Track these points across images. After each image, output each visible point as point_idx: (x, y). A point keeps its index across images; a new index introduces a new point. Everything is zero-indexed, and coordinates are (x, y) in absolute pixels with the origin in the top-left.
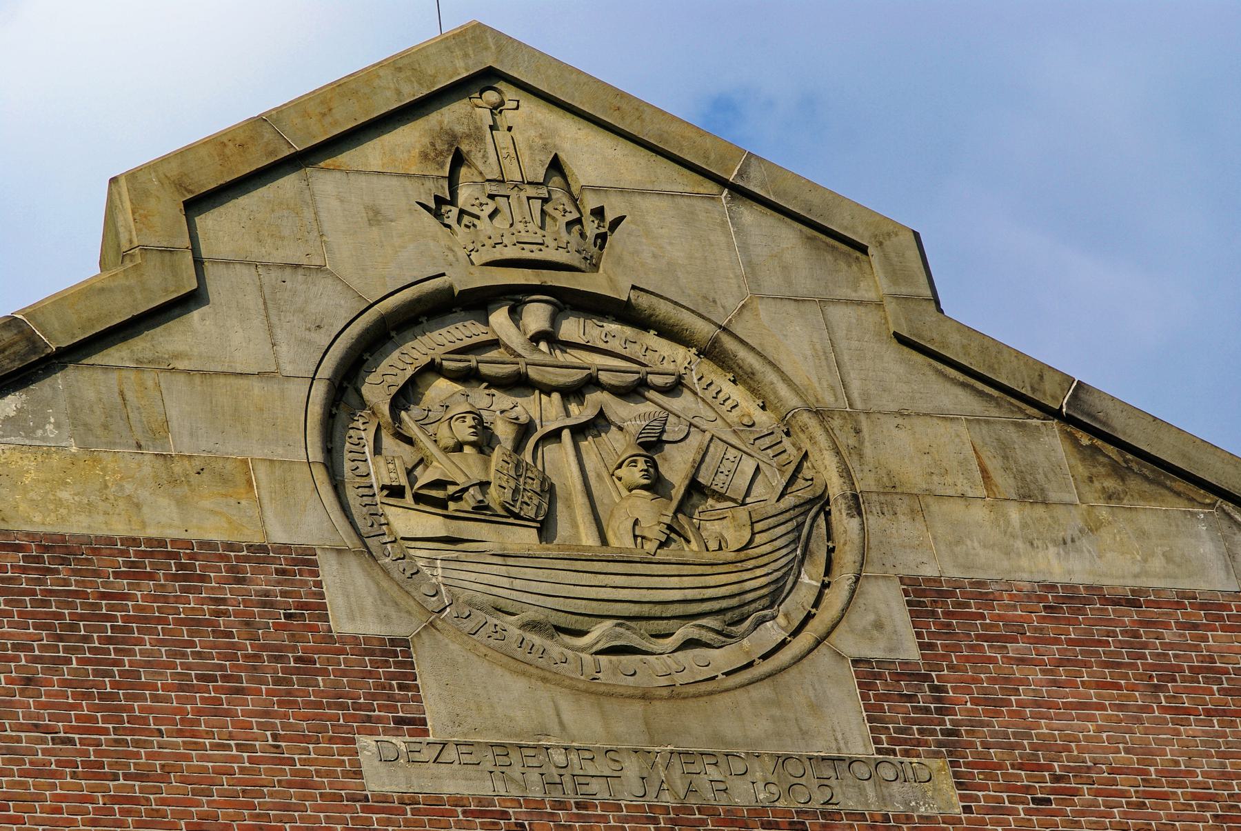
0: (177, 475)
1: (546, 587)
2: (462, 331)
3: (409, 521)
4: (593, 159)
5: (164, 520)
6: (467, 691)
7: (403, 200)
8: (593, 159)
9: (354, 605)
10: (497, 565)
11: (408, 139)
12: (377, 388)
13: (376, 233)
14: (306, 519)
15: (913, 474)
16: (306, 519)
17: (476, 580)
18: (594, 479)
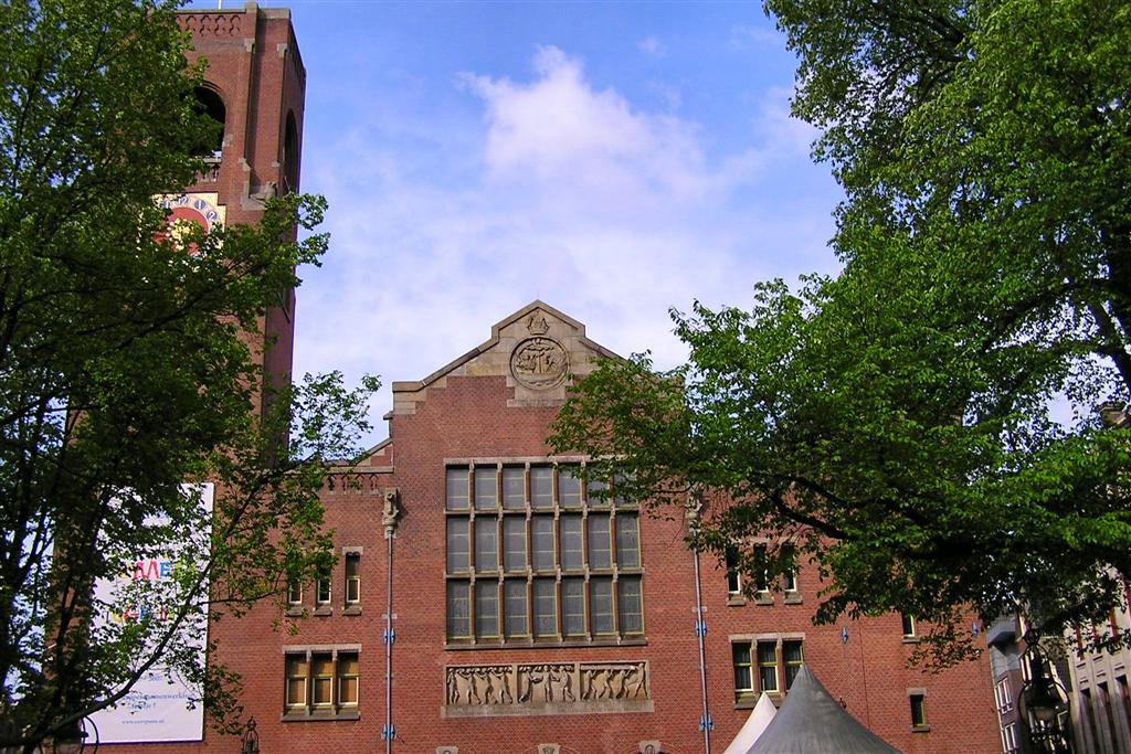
0: (493, 367)
1: (531, 379)
2: (529, 343)
3: (518, 370)
4: (549, 318)
5: (491, 373)
6: (521, 393)
7: (524, 326)
8: (549, 318)
9: (510, 383)
10: (527, 376)
11: (527, 317)
12: (518, 352)
13: (520, 332)
14: (505, 372)
15: (577, 360)
16: (505, 372)
17: (525, 377)
18: (540, 361)
